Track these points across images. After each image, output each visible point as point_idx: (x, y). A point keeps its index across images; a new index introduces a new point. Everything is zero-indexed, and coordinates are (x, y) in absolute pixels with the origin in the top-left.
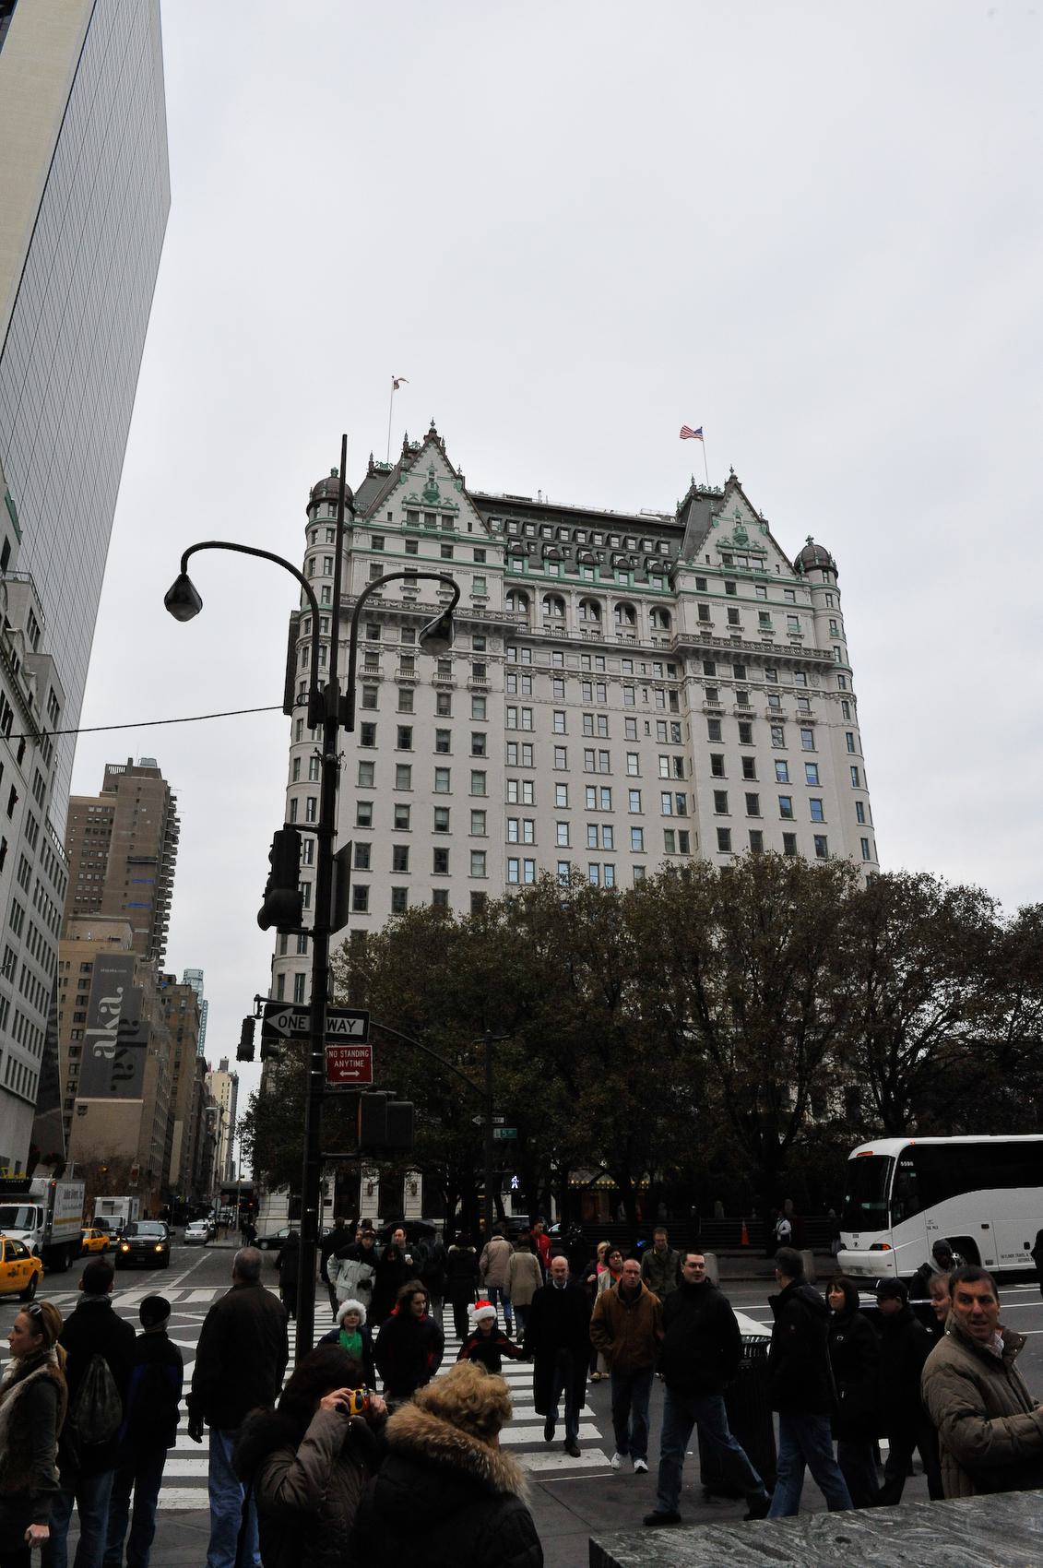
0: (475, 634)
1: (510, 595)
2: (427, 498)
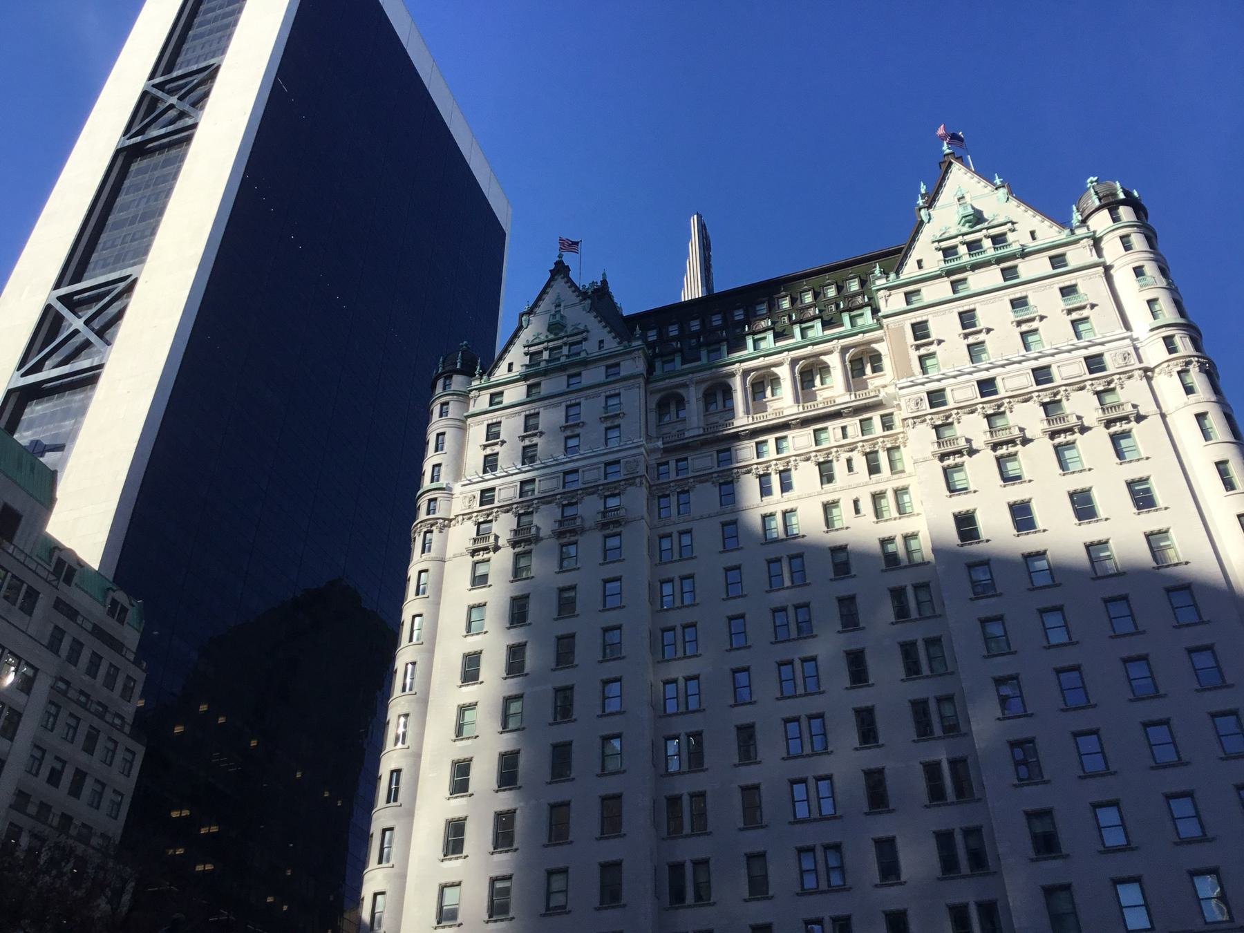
2: (551, 333)
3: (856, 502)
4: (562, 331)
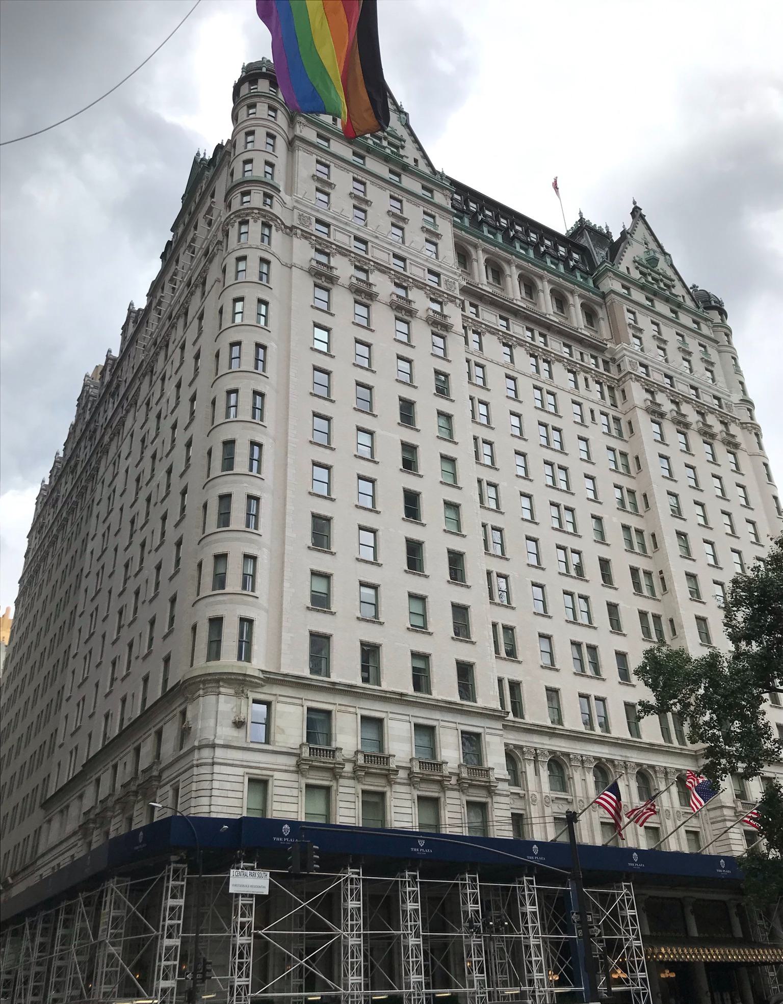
3: (592, 411)
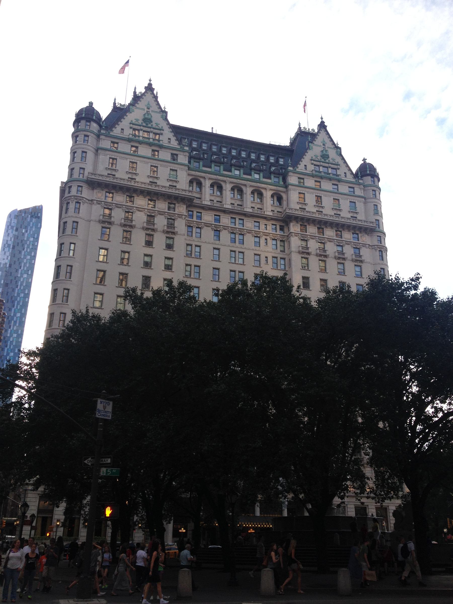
0: (169, 201)
1: (191, 182)
2: (145, 122)
4: (150, 123)
